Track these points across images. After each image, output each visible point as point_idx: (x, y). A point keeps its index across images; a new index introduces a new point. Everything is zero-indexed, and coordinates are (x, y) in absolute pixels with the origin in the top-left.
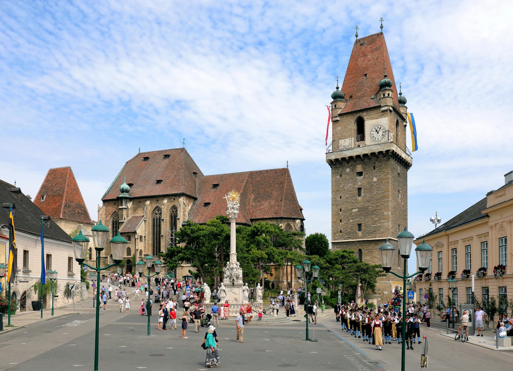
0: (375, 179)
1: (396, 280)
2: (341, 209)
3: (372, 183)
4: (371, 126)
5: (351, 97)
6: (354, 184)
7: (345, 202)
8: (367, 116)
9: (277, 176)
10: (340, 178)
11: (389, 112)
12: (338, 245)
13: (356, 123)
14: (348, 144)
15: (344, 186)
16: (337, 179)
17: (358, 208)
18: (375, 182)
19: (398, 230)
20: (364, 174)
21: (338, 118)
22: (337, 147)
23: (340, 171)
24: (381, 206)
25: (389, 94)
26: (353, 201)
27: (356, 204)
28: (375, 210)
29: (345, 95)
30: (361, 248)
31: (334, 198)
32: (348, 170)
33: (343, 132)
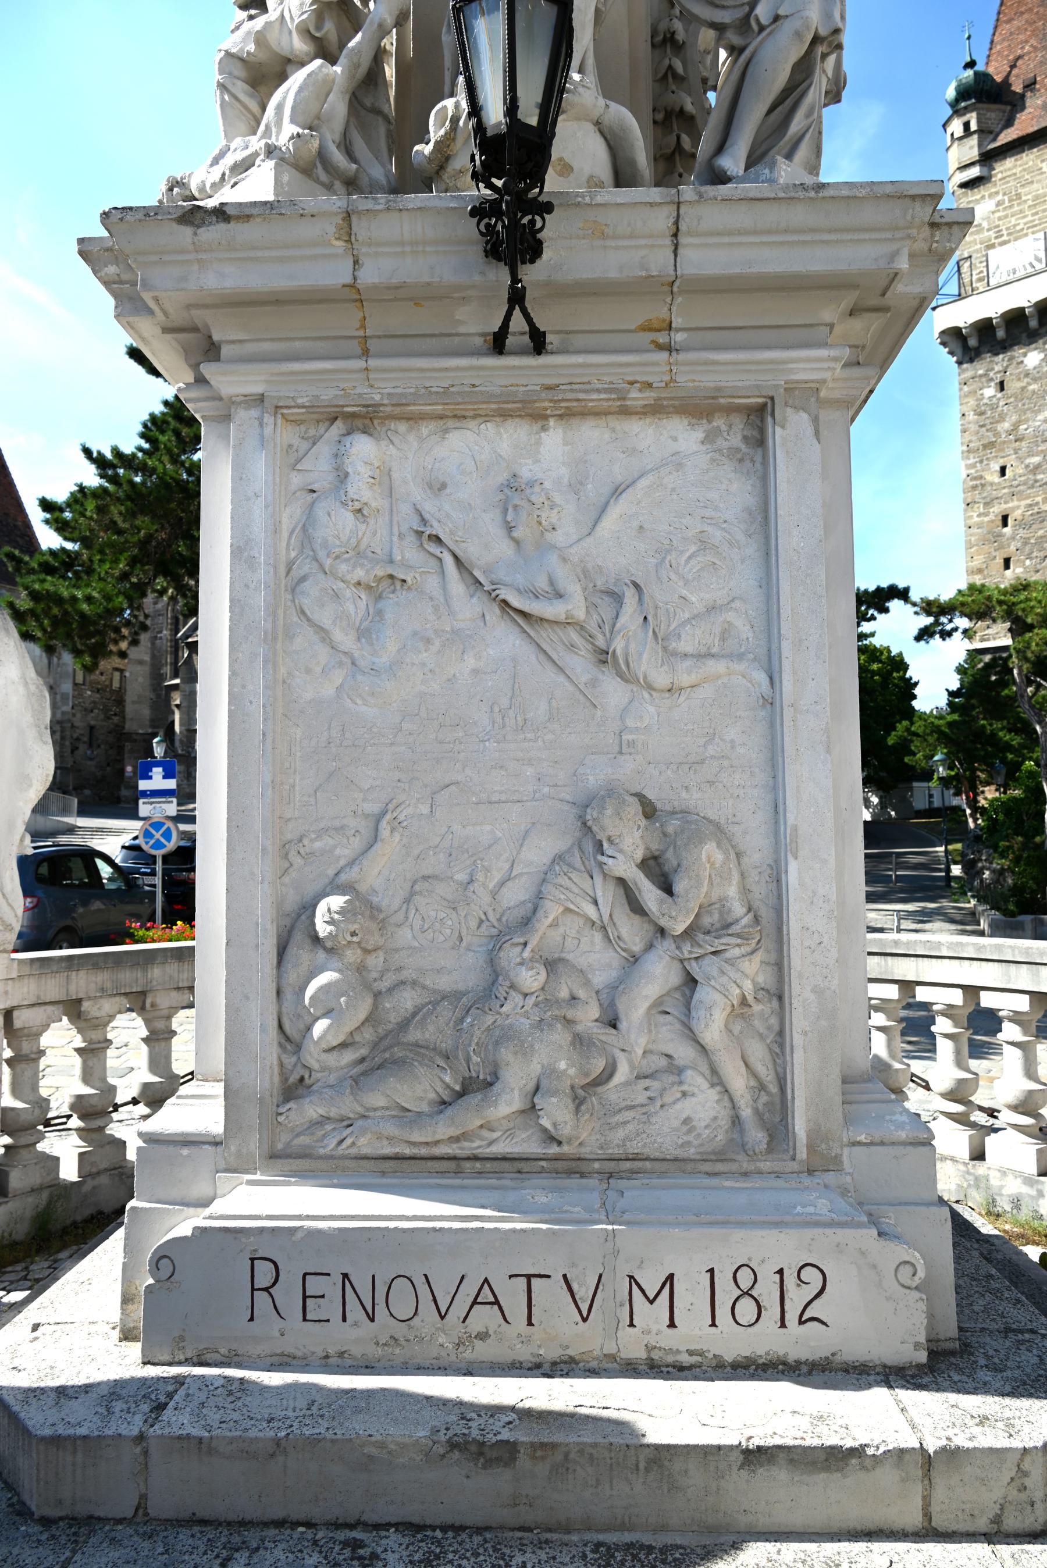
7: (1021, 488)
10: (999, 395)
15: (1016, 426)
16: (985, 401)
23: (997, 368)
31: (975, 478)
33: (1006, 217)
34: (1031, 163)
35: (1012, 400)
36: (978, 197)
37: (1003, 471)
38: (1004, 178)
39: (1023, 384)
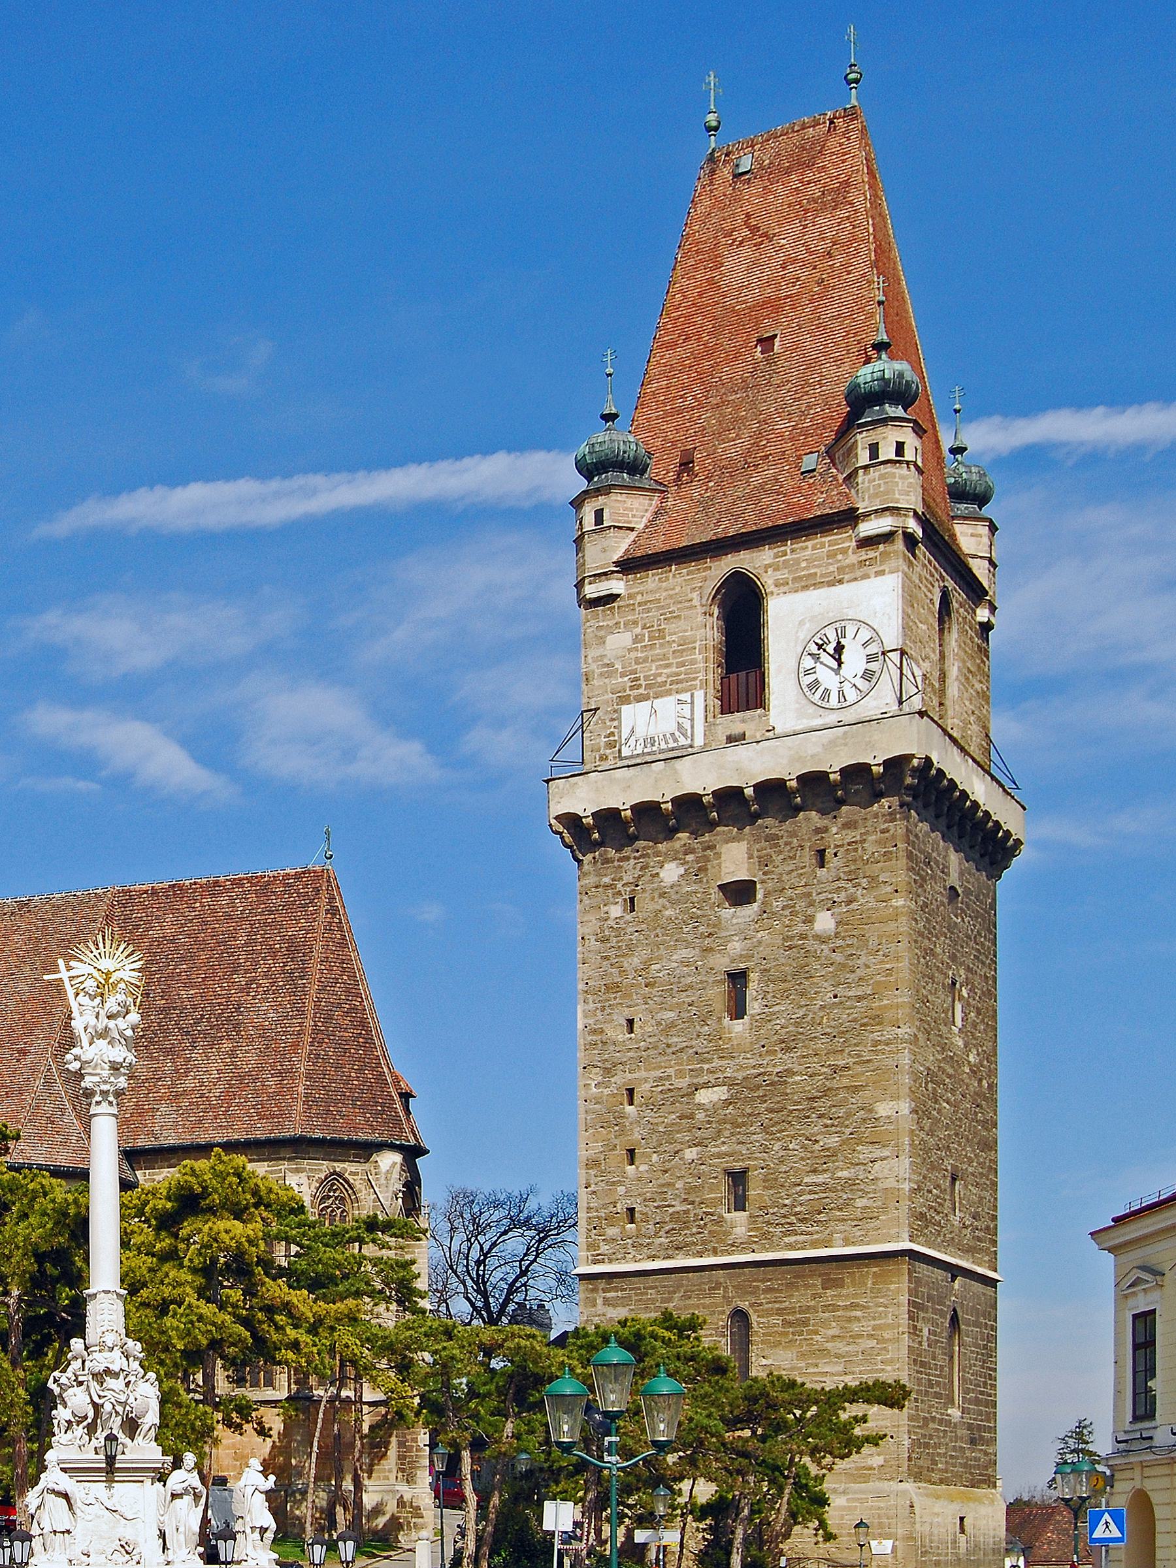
0: (825, 922)
1: (935, 1477)
2: (631, 1092)
3: (812, 944)
4: (801, 623)
5: (686, 464)
6: (707, 950)
7: (651, 1052)
8: (776, 569)
9: (271, 912)
10: (628, 917)
11: (899, 545)
12: (616, 1289)
13: (716, 612)
14: (673, 727)
15: (647, 964)
16: (611, 923)
17: (730, 1083)
18: (822, 939)
19: (948, 1204)
20: (760, 896)
21: (617, 585)
22: (611, 745)
23: (628, 878)
24: (859, 1069)
25: (900, 448)
26: (700, 1044)
27: (717, 1063)
28: (826, 1092)
29: (650, 455)
30: (744, 1305)
31: (593, 1032)
32: (671, 873)
33: (645, 660)
34: (678, 589)
35: (644, 926)
36: (611, 623)
37: (631, 1022)
38: (646, 603)
39: (659, 908)
